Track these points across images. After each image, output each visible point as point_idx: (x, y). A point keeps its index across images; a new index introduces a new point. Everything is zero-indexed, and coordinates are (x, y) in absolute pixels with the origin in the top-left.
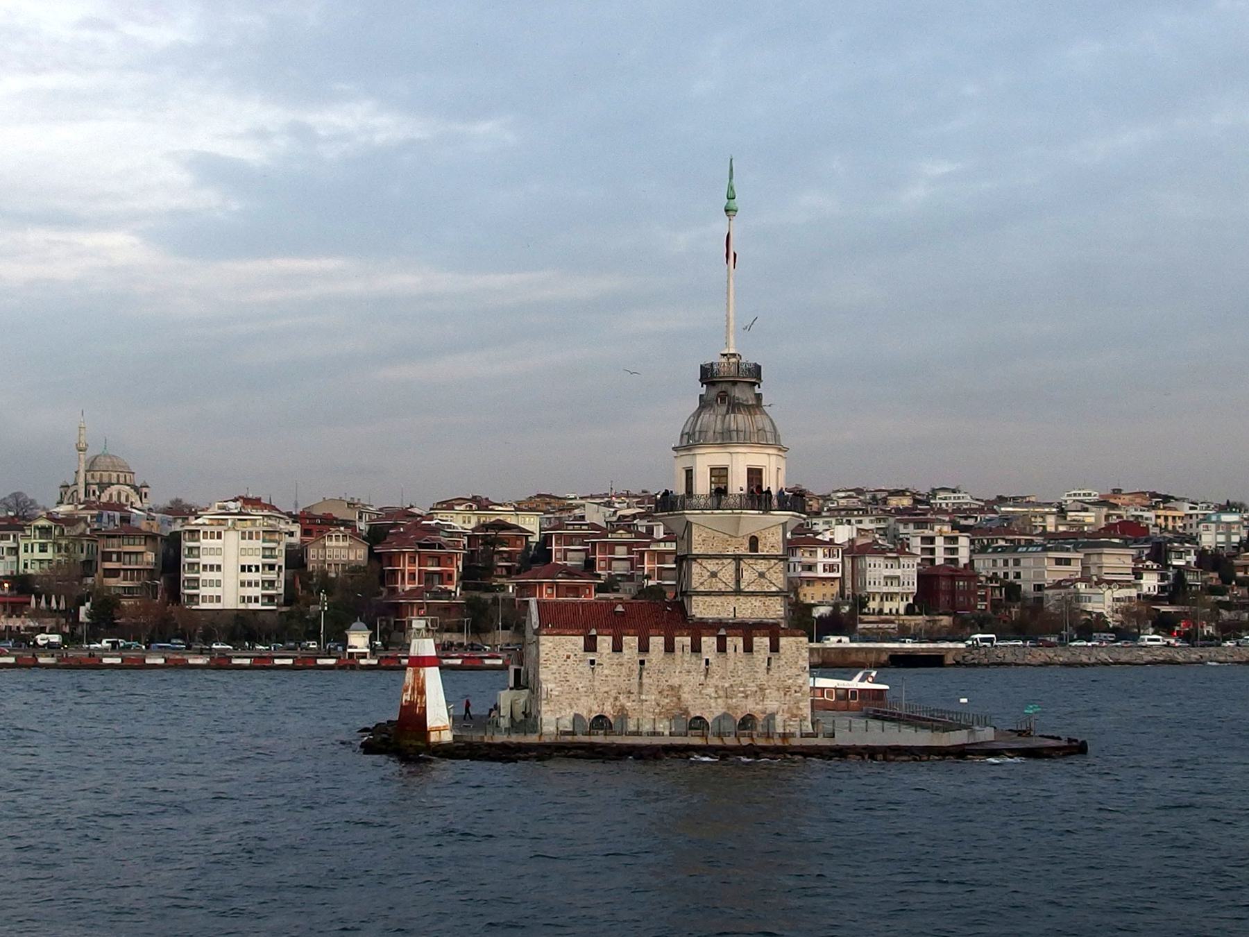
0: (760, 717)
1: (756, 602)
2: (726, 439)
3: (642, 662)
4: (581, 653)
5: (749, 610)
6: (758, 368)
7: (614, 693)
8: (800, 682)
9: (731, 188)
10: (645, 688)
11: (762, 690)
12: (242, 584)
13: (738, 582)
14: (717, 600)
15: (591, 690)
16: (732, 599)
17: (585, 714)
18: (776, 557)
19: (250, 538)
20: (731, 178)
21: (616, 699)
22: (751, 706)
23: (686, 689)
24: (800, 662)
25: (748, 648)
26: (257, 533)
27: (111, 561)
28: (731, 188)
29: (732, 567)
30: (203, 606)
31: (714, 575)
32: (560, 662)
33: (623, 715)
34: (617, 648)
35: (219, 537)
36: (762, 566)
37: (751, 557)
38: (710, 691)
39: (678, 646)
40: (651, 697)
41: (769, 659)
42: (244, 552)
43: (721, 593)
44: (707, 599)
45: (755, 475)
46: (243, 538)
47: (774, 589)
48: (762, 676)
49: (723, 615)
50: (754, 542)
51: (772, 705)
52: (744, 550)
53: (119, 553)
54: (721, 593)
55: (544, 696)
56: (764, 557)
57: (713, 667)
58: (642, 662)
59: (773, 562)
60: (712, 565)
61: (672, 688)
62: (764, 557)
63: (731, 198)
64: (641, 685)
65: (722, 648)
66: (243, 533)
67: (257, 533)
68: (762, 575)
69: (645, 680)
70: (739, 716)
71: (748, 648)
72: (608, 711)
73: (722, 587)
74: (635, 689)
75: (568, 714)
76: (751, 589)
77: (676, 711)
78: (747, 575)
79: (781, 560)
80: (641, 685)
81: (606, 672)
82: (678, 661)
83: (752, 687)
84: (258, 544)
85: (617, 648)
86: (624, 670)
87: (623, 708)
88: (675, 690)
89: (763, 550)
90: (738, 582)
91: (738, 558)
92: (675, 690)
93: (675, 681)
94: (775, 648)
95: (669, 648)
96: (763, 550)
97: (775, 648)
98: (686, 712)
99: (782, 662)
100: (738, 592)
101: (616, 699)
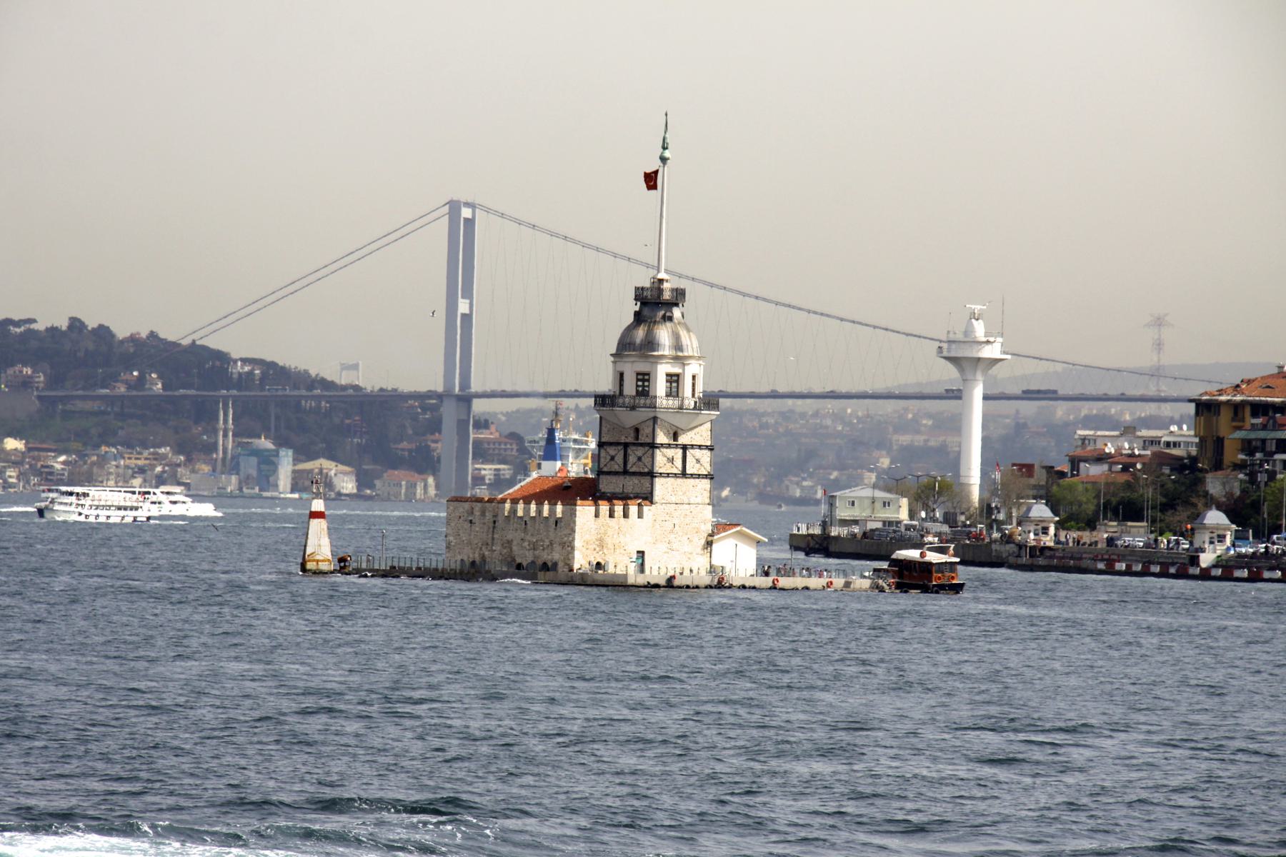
1: (635, 480)
14: (614, 479)
15: (470, 543)
22: (546, 556)
29: (622, 452)
38: (526, 544)
40: (497, 548)
43: (616, 473)
50: (637, 430)
52: (630, 440)
54: (616, 473)
56: (642, 445)
60: (612, 451)
62: (642, 445)
70: (540, 562)
85: (483, 513)
88: (510, 542)
91: (626, 445)
92: (510, 542)
93: (510, 537)
98: (514, 560)
100: (625, 472)
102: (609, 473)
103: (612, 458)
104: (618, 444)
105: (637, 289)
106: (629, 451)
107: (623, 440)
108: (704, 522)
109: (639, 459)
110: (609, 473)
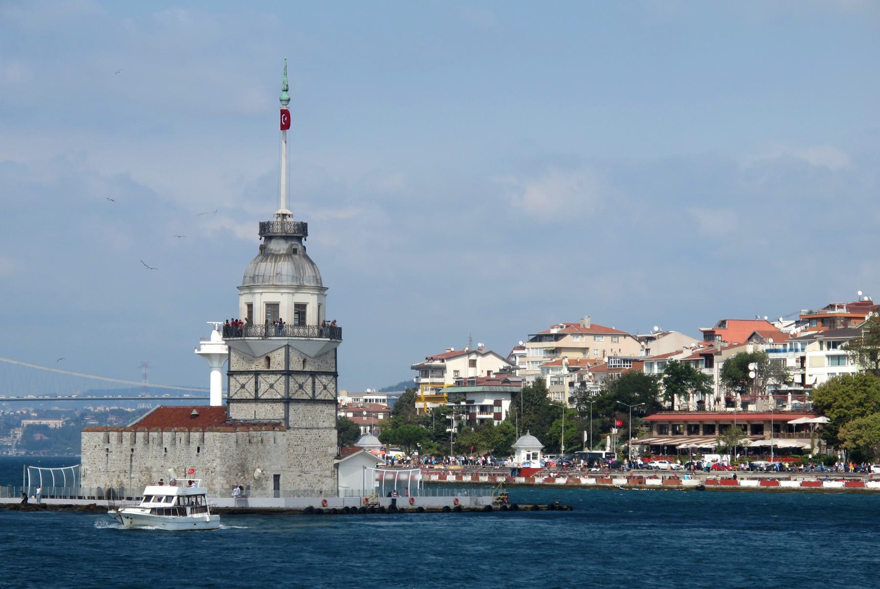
1: (268, 406)
3: (132, 450)
4: (102, 444)
5: (265, 412)
7: (117, 473)
8: (214, 465)
10: (133, 469)
13: (256, 391)
16: (253, 405)
17: (102, 487)
21: (119, 476)
23: (154, 469)
24: (216, 451)
25: (188, 442)
29: (253, 380)
32: (92, 450)
33: (122, 489)
34: (120, 440)
36: (272, 379)
37: (265, 372)
39: (151, 439)
41: (199, 449)
43: (246, 401)
45: (273, 308)
47: (279, 397)
49: (248, 417)
50: (268, 359)
52: (261, 366)
54: (246, 401)
55: (83, 474)
57: (169, 454)
58: (132, 450)
59: (278, 376)
60: (242, 379)
64: (131, 466)
69: (134, 464)
71: (188, 442)
72: (115, 486)
73: (247, 396)
74: (128, 468)
78: (263, 387)
79: (283, 374)
80: (131, 466)
81: (114, 457)
82: (151, 449)
85: (120, 440)
86: (123, 456)
87: (122, 483)
90: (256, 391)
91: (257, 373)
93: (149, 464)
95: (147, 440)
97: (203, 440)
99: (205, 451)
100: (257, 400)
101: (119, 476)
103: (243, 386)
108: (331, 445)
109: (272, 386)
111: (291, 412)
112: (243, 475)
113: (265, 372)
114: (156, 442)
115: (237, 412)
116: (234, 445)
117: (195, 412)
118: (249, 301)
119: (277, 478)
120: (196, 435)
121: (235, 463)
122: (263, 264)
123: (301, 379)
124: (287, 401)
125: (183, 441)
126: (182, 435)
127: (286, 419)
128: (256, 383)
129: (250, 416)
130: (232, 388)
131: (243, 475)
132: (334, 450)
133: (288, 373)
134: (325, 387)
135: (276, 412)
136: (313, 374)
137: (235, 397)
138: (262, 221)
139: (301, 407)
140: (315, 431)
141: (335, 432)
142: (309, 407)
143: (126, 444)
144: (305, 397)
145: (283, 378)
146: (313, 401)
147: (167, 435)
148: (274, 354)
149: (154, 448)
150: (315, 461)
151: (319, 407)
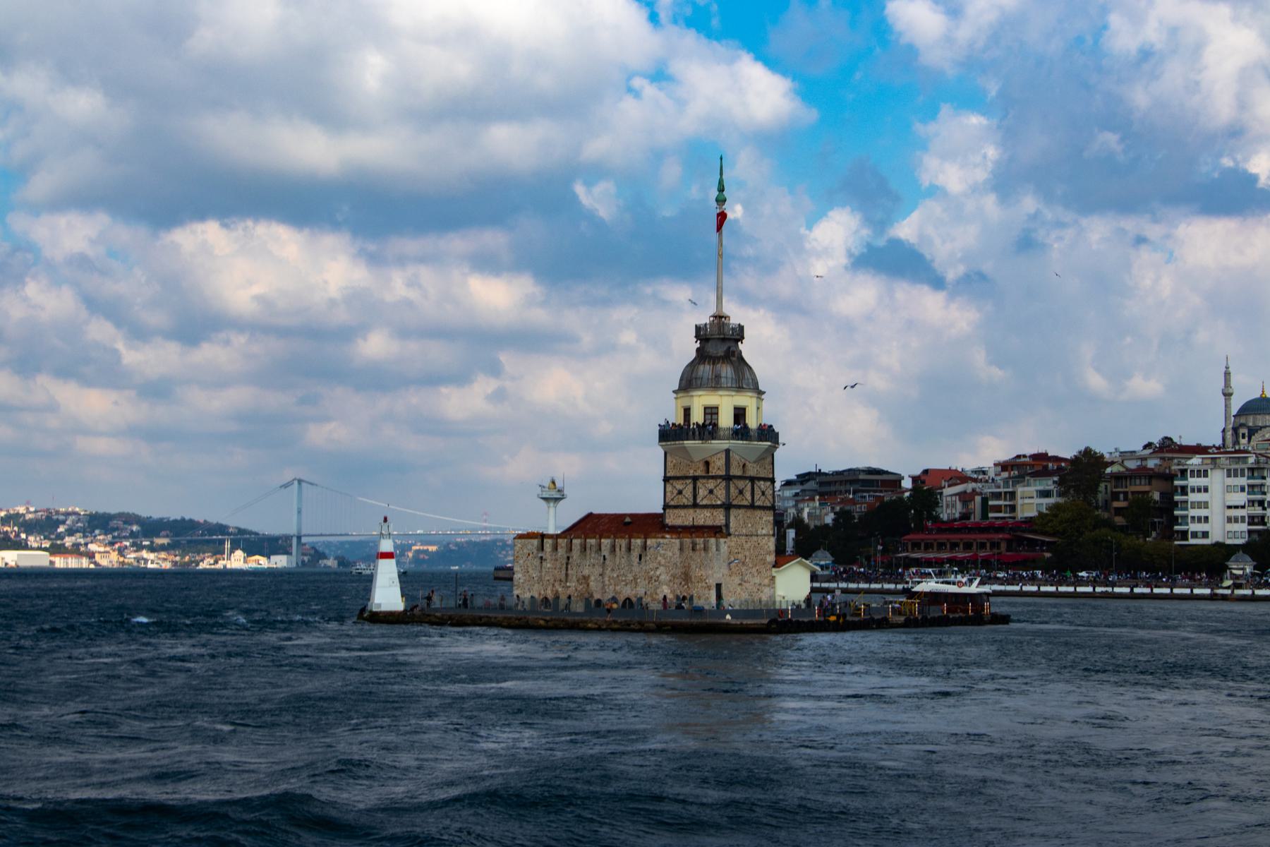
0: (634, 600)
1: (707, 513)
2: (715, 384)
5: (703, 518)
6: (741, 328)
9: (721, 183)
11: (635, 579)
12: (1206, 519)
14: (682, 512)
15: (540, 579)
16: (691, 511)
18: (720, 477)
19: (1236, 476)
20: (721, 174)
22: (627, 592)
25: (629, 549)
26: (1243, 470)
27: (1118, 499)
28: (721, 183)
29: (691, 486)
30: (1192, 541)
31: (680, 492)
35: (1206, 475)
36: (711, 484)
37: (704, 477)
40: (572, 584)
42: (1229, 489)
44: (676, 511)
46: (1229, 476)
48: (636, 569)
49: (686, 523)
50: (707, 464)
51: (640, 591)
52: (699, 473)
53: (1126, 494)
54: (685, 507)
56: (713, 477)
57: (607, 562)
61: (584, 577)
62: (713, 477)
63: (721, 189)
64: (567, 575)
65: (613, 549)
66: (1229, 471)
67: (1243, 470)
68: (711, 492)
70: (621, 599)
71: (629, 549)
72: (550, 595)
73: (685, 501)
75: (528, 595)
76: (705, 502)
77: (586, 595)
78: (702, 492)
80: (567, 575)
83: (630, 577)
84: (1243, 481)
88: (586, 578)
89: (713, 472)
91: (695, 479)
92: (586, 578)
93: (586, 572)
94: (645, 547)
95: (584, 548)
96: (713, 472)
97: (645, 547)
98: (592, 596)
100: (695, 505)
102: (676, 507)
103: (680, 492)
104: (687, 478)
105: (698, 329)
106: (699, 484)
107: (691, 473)
108: (769, 553)
109: (711, 492)
110: (676, 507)
111: (732, 518)
112: (687, 584)
113: (704, 477)
114: (594, 549)
115: (673, 519)
116: (678, 552)
117: (628, 520)
118: (686, 404)
119: (719, 586)
120: (638, 542)
121: (679, 572)
122: (701, 367)
123: (741, 484)
124: (727, 507)
125: (623, 549)
126: (622, 543)
127: (727, 525)
128: (695, 488)
129: (688, 523)
130: (668, 494)
131: (687, 584)
132: (771, 558)
133: (728, 478)
134: (763, 493)
135: (718, 518)
136: (753, 480)
137: (672, 503)
138: (698, 323)
139: (741, 511)
140: (755, 538)
141: (773, 540)
142: (749, 513)
143: (562, 552)
144: (745, 503)
145: (724, 484)
146: (752, 506)
147: (606, 542)
148: (714, 458)
149: (593, 558)
150: (754, 570)
151: (759, 513)
